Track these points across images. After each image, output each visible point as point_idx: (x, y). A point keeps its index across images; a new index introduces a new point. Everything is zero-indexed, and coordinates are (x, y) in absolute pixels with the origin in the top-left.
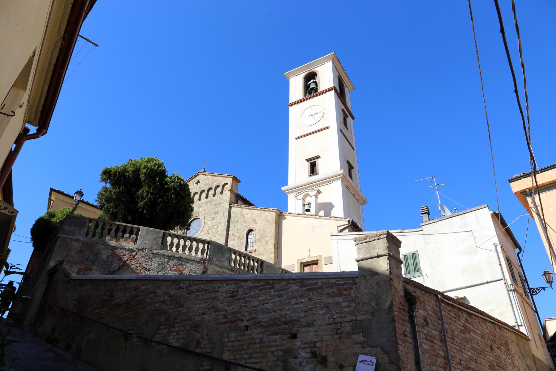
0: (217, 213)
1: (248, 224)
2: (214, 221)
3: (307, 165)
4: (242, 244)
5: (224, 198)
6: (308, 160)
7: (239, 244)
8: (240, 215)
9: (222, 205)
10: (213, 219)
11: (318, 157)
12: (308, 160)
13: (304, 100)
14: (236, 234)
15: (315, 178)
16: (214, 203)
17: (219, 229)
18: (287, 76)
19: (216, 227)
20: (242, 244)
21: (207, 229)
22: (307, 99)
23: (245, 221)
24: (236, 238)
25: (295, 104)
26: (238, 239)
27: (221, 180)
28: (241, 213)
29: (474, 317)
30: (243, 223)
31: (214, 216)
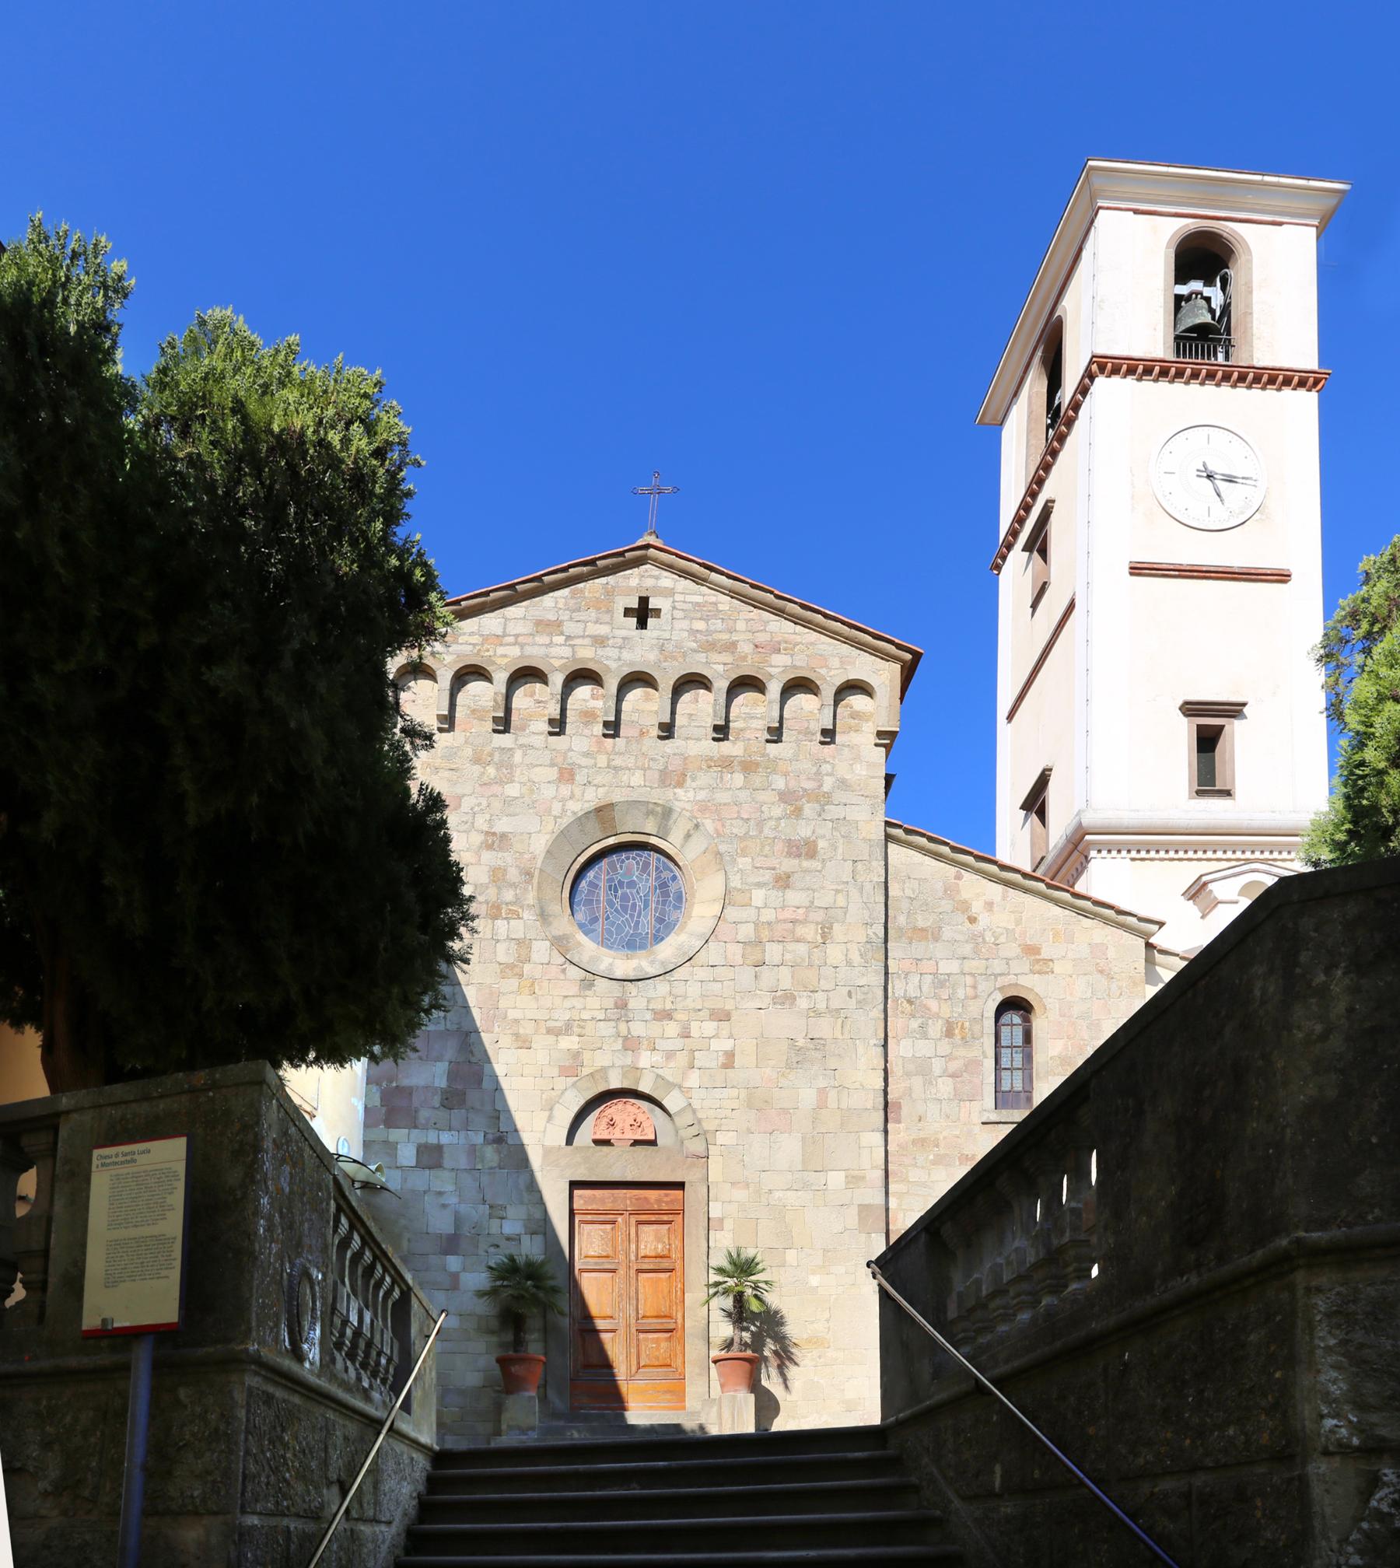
0: (806, 849)
1: (998, 966)
2: (794, 897)
3: (1184, 732)
4: (972, 1065)
5: (842, 770)
6: (1190, 709)
7: (954, 1066)
8: (946, 905)
9: (833, 812)
10: (783, 882)
11: (1234, 710)
12: (1190, 709)
13: (1164, 373)
14: (933, 1005)
15: (1213, 811)
16: (780, 783)
17: (835, 954)
18: (1097, 182)
19: (810, 932)
20: (972, 1065)
21: (746, 932)
22: (1180, 374)
23: (977, 939)
24: (936, 1029)
25: (1131, 371)
26: (949, 1033)
27: (835, 660)
28: (950, 891)
29: (1142, 1546)
30: (967, 949)
31: (788, 864)
